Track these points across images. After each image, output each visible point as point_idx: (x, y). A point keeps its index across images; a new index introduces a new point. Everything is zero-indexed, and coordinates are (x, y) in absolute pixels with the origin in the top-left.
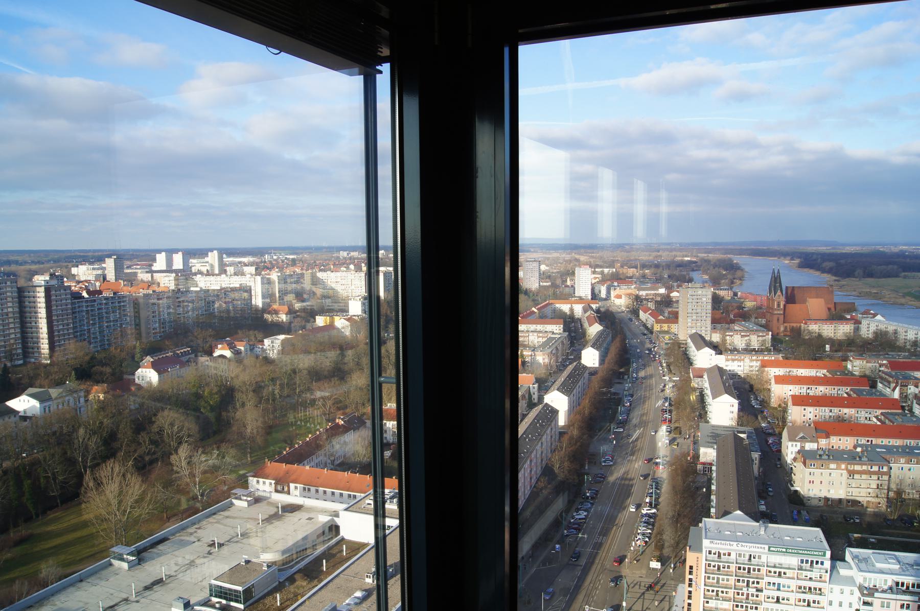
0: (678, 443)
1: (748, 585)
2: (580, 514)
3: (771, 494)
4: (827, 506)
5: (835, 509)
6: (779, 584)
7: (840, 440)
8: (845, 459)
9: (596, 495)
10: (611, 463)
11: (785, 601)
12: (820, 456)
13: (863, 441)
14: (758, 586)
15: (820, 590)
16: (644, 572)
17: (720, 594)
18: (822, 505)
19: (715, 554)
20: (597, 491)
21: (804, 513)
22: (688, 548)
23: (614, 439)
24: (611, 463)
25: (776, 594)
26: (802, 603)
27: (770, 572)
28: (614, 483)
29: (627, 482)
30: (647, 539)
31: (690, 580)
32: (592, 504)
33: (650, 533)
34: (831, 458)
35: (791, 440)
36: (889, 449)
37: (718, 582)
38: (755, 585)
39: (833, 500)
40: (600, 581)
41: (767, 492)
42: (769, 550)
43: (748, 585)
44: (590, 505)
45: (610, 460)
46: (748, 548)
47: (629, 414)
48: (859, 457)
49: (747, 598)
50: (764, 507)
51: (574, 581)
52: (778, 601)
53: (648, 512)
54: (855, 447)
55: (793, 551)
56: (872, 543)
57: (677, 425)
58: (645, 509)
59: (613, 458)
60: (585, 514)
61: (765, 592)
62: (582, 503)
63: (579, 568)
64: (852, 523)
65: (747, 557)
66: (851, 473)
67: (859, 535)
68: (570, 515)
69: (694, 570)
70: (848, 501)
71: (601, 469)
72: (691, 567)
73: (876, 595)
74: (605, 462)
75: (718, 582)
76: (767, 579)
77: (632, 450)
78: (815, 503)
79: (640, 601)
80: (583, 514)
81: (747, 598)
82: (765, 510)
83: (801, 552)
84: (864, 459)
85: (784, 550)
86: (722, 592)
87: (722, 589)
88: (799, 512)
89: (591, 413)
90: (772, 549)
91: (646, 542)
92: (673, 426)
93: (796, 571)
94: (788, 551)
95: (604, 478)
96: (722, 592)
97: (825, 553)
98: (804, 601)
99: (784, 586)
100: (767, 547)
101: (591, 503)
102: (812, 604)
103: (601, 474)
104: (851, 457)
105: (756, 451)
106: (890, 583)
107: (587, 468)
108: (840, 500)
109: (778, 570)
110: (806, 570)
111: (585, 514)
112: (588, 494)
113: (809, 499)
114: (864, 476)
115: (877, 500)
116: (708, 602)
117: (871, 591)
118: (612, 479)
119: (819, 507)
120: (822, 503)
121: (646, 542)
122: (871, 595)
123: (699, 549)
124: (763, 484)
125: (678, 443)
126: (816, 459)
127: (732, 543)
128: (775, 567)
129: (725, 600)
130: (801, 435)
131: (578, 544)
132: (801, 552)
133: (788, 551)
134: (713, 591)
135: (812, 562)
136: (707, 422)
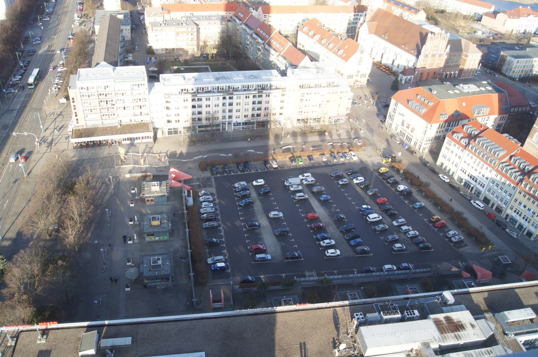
0: (85, 25)
1: (107, 103)
2: (16, 78)
3: (137, 50)
4: (167, 53)
5: (171, 54)
6: (123, 100)
7: (176, 14)
8: (174, 25)
9: (28, 64)
10: (40, 42)
11: (144, 107)
12: (161, 24)
13: (188, 14)
14: (112, 102)
15: (145, 99)
16: (57, 106)
17: (92, 110)
18: (164, 53)
19: (85, 89)
20: (29, 61)
21: (153, 58)
22: (68, 88)
23: (41, 25)
24: (40, 42)
25: (122, 105)
26: (137, 108)
27: (117, 94)
28: (41, 55)
29: (50, 53)
30: (59, 87)
31: (74, 106)
32: (25, 70)
33: (62, 83)
34: (166, 25)
35: (148, 16)
36: (199, 18)
37: (90, 104)
38: (111, 102)
39: (170, 50)
40: (28, 116)
41: (134, 49)
42: (114, 82)
43: (107, 103)
44: (23, 71)
45: (39, 40)
46: (103, 83)
47: (54, 8)
48: (182, 24)
49: (108, 110)
50: (131, 58)
51: (12, 120)
52: (124, 108)
53: (62, 70)
54: (182, 18)
55: (128, 80)
56: (182, 70)
57: (86, 12)
58: (59, 68)
59: (41, 38)
60: (20, 77)
61: (116, 105)
62: (18, 70)
63: (16, 111)
64: (178, 61)
65: (103, 88)
66: (178, 34)
67: (177, 67)
68: (10, 80)
69: (75, 100)
70: (178, 49)
71: (33, 47)
72: (73, 99)
73: (172, 97)
74: (35, 42)
75: (90, 104)
76: (116, 98)
77: (54, 32)
78: (160, 52)
79: (54, 123)
80: (18, 77)
81: (108, 110)
82: (132, 59)
83: (131, 80)
84: (184, 24)
85: (122, 81)
86: (94, 109)
87: (94, 108)
88: (151, 58)
89: (21, 9)
90: (115, 81)
91: (59, 89)
92: (83, 13)
93: (131, 91)
94: (125, 80)
95: (34, 53)
96: (94, 109)
97: (144, 79)
98: (138, 106)
99: (126, 100)
100: (113, 80)
101: (24, 70)
102: (142, 107)
103: (32, 50)
104: (179, 24)
105: (129, 25)
106: (180, 91)
107: (22, 47)
108: (173, 49)
109: (121, 92)
110: (136, 90)
111: (20, 77)
112: (22, 64)
113: (157, 50)
114: (185, 34)
115: (192, 47)
116: (87, 116)
117: (169, 95)
118: (40, 52)
119: (163, 54)
120: (164, 52)
121: (59, 89)
122: (169, 97)
123: (75, 88)
124: (133, 44)
125: (85, 25)
126: (158, 26)
127: (92, 81)
128: (119, 90)
129: (96, 113)
130: (154, 13)
131: (15, 97)
132: (131, 80)
133: (125, 80)
134: (89, 110)
135: (138, 85)
136: (104, 9)
